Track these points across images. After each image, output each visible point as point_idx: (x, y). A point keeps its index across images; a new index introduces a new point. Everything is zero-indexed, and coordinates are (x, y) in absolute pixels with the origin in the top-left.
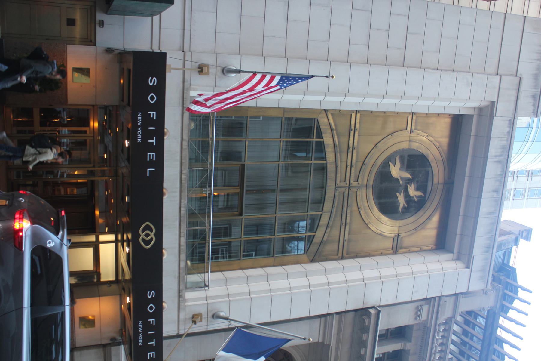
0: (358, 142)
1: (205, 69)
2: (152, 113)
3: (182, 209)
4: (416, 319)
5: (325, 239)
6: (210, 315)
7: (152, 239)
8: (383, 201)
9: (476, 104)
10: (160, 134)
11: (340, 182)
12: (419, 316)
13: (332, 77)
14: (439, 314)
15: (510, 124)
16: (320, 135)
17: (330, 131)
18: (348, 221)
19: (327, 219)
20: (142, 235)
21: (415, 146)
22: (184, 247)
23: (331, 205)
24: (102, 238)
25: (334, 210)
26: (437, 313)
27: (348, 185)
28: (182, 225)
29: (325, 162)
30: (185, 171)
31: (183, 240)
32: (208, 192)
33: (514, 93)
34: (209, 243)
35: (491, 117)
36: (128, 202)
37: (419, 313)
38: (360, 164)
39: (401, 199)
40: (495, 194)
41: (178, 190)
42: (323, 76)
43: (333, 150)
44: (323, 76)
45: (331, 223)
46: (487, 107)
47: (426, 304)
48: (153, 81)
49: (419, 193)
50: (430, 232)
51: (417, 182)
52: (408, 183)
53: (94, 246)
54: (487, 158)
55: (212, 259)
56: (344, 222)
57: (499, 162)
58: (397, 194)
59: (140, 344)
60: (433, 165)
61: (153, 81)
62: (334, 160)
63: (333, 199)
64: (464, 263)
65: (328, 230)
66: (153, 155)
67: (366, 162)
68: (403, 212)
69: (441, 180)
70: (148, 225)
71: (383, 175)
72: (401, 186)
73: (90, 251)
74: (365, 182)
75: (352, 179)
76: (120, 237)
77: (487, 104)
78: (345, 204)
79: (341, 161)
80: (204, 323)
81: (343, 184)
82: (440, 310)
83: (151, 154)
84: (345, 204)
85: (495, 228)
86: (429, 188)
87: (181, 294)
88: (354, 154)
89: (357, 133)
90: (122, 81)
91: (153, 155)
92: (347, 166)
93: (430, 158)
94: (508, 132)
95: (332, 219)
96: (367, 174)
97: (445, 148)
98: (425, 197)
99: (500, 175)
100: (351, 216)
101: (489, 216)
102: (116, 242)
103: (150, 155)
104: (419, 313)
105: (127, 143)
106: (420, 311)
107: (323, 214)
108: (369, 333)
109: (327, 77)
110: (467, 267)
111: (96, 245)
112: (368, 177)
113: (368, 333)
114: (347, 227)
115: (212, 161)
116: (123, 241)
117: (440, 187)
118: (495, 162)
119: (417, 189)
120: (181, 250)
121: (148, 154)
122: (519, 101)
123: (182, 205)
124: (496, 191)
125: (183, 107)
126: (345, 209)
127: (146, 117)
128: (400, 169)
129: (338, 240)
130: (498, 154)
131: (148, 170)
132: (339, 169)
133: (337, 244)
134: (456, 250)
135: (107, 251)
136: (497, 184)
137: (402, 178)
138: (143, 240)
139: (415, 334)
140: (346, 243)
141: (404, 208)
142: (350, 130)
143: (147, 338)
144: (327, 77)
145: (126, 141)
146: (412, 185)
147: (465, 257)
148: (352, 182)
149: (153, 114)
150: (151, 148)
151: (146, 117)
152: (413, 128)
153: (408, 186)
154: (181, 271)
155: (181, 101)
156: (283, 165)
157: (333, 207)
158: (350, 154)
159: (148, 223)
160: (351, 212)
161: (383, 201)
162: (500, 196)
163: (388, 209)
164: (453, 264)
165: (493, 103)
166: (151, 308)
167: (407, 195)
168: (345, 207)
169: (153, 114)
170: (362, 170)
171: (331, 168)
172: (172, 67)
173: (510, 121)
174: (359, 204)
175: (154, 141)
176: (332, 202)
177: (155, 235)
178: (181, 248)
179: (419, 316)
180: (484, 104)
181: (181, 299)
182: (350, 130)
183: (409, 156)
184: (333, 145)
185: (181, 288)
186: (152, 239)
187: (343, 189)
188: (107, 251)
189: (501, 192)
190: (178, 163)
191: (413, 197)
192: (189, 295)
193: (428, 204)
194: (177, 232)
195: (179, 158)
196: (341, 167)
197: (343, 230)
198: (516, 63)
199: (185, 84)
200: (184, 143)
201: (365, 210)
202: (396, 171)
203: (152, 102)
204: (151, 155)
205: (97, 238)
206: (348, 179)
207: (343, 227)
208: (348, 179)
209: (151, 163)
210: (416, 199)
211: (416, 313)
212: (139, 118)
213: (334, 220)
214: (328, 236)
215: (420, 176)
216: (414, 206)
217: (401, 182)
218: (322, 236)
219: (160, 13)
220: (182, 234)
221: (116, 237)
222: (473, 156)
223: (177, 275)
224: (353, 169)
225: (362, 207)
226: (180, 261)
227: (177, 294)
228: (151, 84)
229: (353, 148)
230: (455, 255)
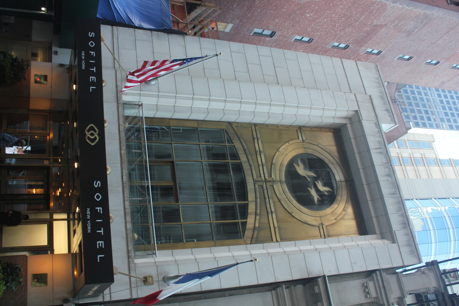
0: (263, 147)
1: (150, 280)
2: (99, 208)
3: (124, 177)
4: (366, 297)
5: (257, 225)
6: (161, 278)
7: (96, 138)
8: (299, 194)
9: (344, 114)
10: (106, 224)
11: (257, 177)
13: (256, 260)
14: (386, 288)
15: (376, 125)
16: (230, 141)
17: (237, 138)
19: (254, 208)
20: (88, 134)
21: (310, 151)
22: (128, 210)
23: (254, 195)
24: (56, 216)
25: (258, 200)
26: (384, 287)
27: (264, 180)
28: (125, 190)
29: (247, 202)
30: (124, 148)
31: (129, 226)
32: (146, 184)
33: (370, 105)
34: (153, 225)
35: (360, 121)
36: (78, 168)
37: (367, 290)
38: (269, 164)
39: (313, 192)
41: (119, 162)
42: (248, 261)
43: (244, 152)
44: (248, 261)
45: (258, 212)
46: (354, 115)
47: (370, 281)
48: (97, 184)
49: (327, 189)
50: (350, 223)
51: (323, 180)
52: (315, 180)
53: (48, 223)
54: (370, 150)
55: (157, 243)
56: (269, 210)
57: (381, 153)
58: (309, 189)
59: (89, 231)
60: (331, 166)
61: (97, 184)
62: (246, 159)
63: (254, 190)
64: (389, 240)
65: (258, 217)
66: (102, 243)
67: (274, 162)
68: (319, 205)
69: (342, 178)
70: (92, 127)
71: (291, 173)
72: (309, 182)
73: (45, 228)
74: (278, 179)
75: (266, 175)
76: (71, 217)
77: (353, 113)
78: (266, 195)
79: (253, 162)
81: (259, 179)
82: (385, 283)
83: (93, 77)
85: (402, 207)
86: (335, 185)
87: (130, 254)
88: (263, 156)
89: (260, 141)
90: (75, 273)
91: (102, 243)
92: (259, 166)
93: (327, 161)
94: (378, 132)
95: (258, 208)
96: (278, 172)
97: (336, 154)
98: (334, 192)
99: (386, 163)
100: (274, 206)
101: (392, 196)
102: (68, 220)
103: (92, 78)
105: (76, 165)
106: (366, 287)
107: (249, 203)
108: (322, 301)
109: (251, 261)
110: (394, 242)
111: (50, 221)
112: (279, 174)
114: (274, 215)
115: (146, 156)
116: (74, 219)
117: (344, 184)
118: (377, 153)
119: (325, 185)
120: (127, 213)
121: (98, 242)
122: (376, 110)
123: (124, 174)
124: (389, 175)
125: (118, 103)
126: (267, 200)
127: (94, 212)
128: (304, 169)
129: (268, 227)
130: (377, 147)
131: (99, 256)
132: (253, 167)
133: (269, 230)
134: (377, 231)
135: (60, 228)
136: (387, 170)
137: (308, 176)
138: (89, 138)
140: (277, 230)
141: (318, 200)
142: (254, 139)
143: (89, 65)
144: (251, 261)
145: (78, 208)
146: (319, 182)
147: (387, 234)
148: (267, 177)
149: (100, 209)
150: (100, 237)
151: (94, 212)
152: (304, 138)
153: (316, 182)
154: (128, 232)
155: (116, 99)
156: (205, 149)
157: (256, 198)
158: (259, 156)
159: (92, 125)
160: (274, 202)
161: (299, 194)
162: (394, 180)
163: (306, 201)
164: (380, 241)
165: (356, 111)
166: (98, 197)
167: (318, 191)
168: (267, 198)
169: (100, 209)
170: (272, 169)
171: (246, 166)
172: (119, 271)
173: (375, 123)
174: (278, 196)
175: (102, 231)
176: (254, 193)
177: (98, 135)
178: (126, 210)
179: (368, 293)
180: (350, 113)
181: (130, 260)
182: (254, 139)
183: (308, 159)
184: (243, 149)
185: (129, 248)
186: (96, 138)
187: (261, 183)
188: (60, 228)
189: (393, 176)
190: (117, 142)
191: (323, 192)
192: (137, 261)
193: (339, 198)
194: (122, 197)
195: (117, 138)
196: (254, 166)
197: (270, 218)
198: (363, 88)
199: (118, 88)
200: (120, 127)
201: (285, 201)
202: (301, 170)
203: (98, 200)
204: (93, 78)
205: (51, 216)
206: (262, 175)
207: (270, 215)
208: (262, 175)
209: (101, 250)
210: (326, 194)
211: (364, 291)
212: (88, 212)
213: (260, 210)
214: (259, 223)
215: (323, 175)
216: (328, 199)
217: (309, 179)
218: (253, 222)
219: (109, 286)
220: (126, 198)
221: (68, 216)
222: (364, 169)
223: (124, 236)
224: (265, 168)
225: (282, 199)
226: (126, 223)
227: (126, 255)
228: (96, 186)
229: (260, 152)
230: (379, 236)
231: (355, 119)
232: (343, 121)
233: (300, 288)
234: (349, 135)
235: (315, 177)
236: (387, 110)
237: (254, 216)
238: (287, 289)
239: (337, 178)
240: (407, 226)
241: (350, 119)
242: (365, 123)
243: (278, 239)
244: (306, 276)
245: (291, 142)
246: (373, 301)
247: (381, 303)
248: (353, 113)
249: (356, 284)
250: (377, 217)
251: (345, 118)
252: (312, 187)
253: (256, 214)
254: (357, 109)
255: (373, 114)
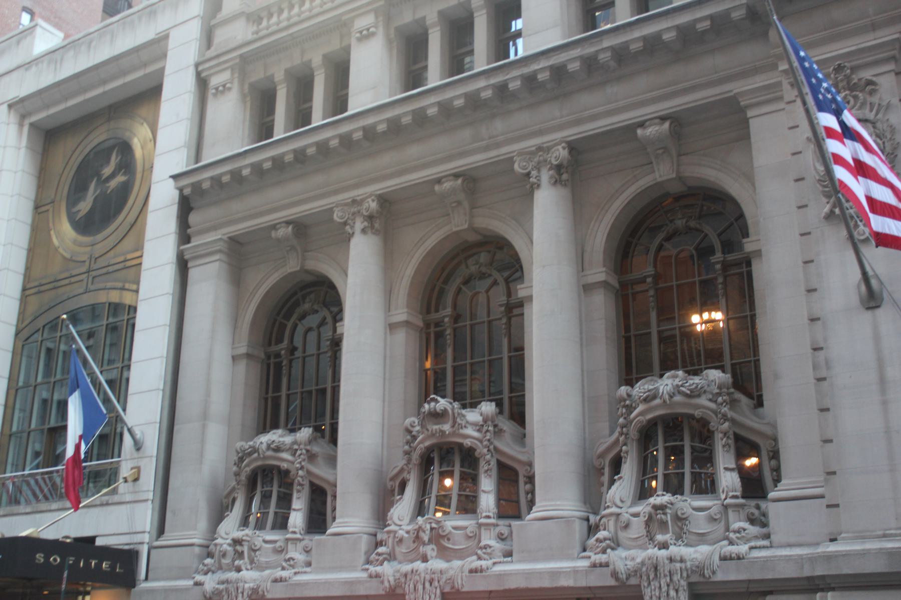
4: (230, 89)
6: (136, 454)
9: (13, 129)
12: (224, 86)
18: (122, 259)
23: (101, 292)
35: (22, 100)
39: (113, 184)
40: (94, 44)
45: (120, 285)
65: (127, 286)
74: (89, 249)
78: (105, 270)
80: (142, 464)
84: (105, 270)
104: (221, 88)
113: (199, 183)
114: (129, 257)
137: (94, 192)
139: (257, 74)
141: (125, 174)
165: (10, 106)
180: (13, 118)
202: (84, 206)
207: (129, 264)
211: (223, 92)
220: (48, 508)
224: (74, 273)
227: (105, 508)
231: (20, 107)
232: (26, 129)
233: (193, 218)
234: (44, 118)
235: (98, 180)
236: (18, 42)
237: (125, 293)
238: (193, 239)
239: (103, 137)
240: (154, 7)
241: (23, 117)
242: (23, 93)
243: (138, 254)
244: (174, 210)
245: (51, 225)
246: (236, 75)
247: (237, 61)
248: (12, 112)
249: (213, 107)
250: (145, 65)
251: (21, 125)
252: (108, 185)
253: (123, 289)
254: (5, 106)
255: (15, 75)
